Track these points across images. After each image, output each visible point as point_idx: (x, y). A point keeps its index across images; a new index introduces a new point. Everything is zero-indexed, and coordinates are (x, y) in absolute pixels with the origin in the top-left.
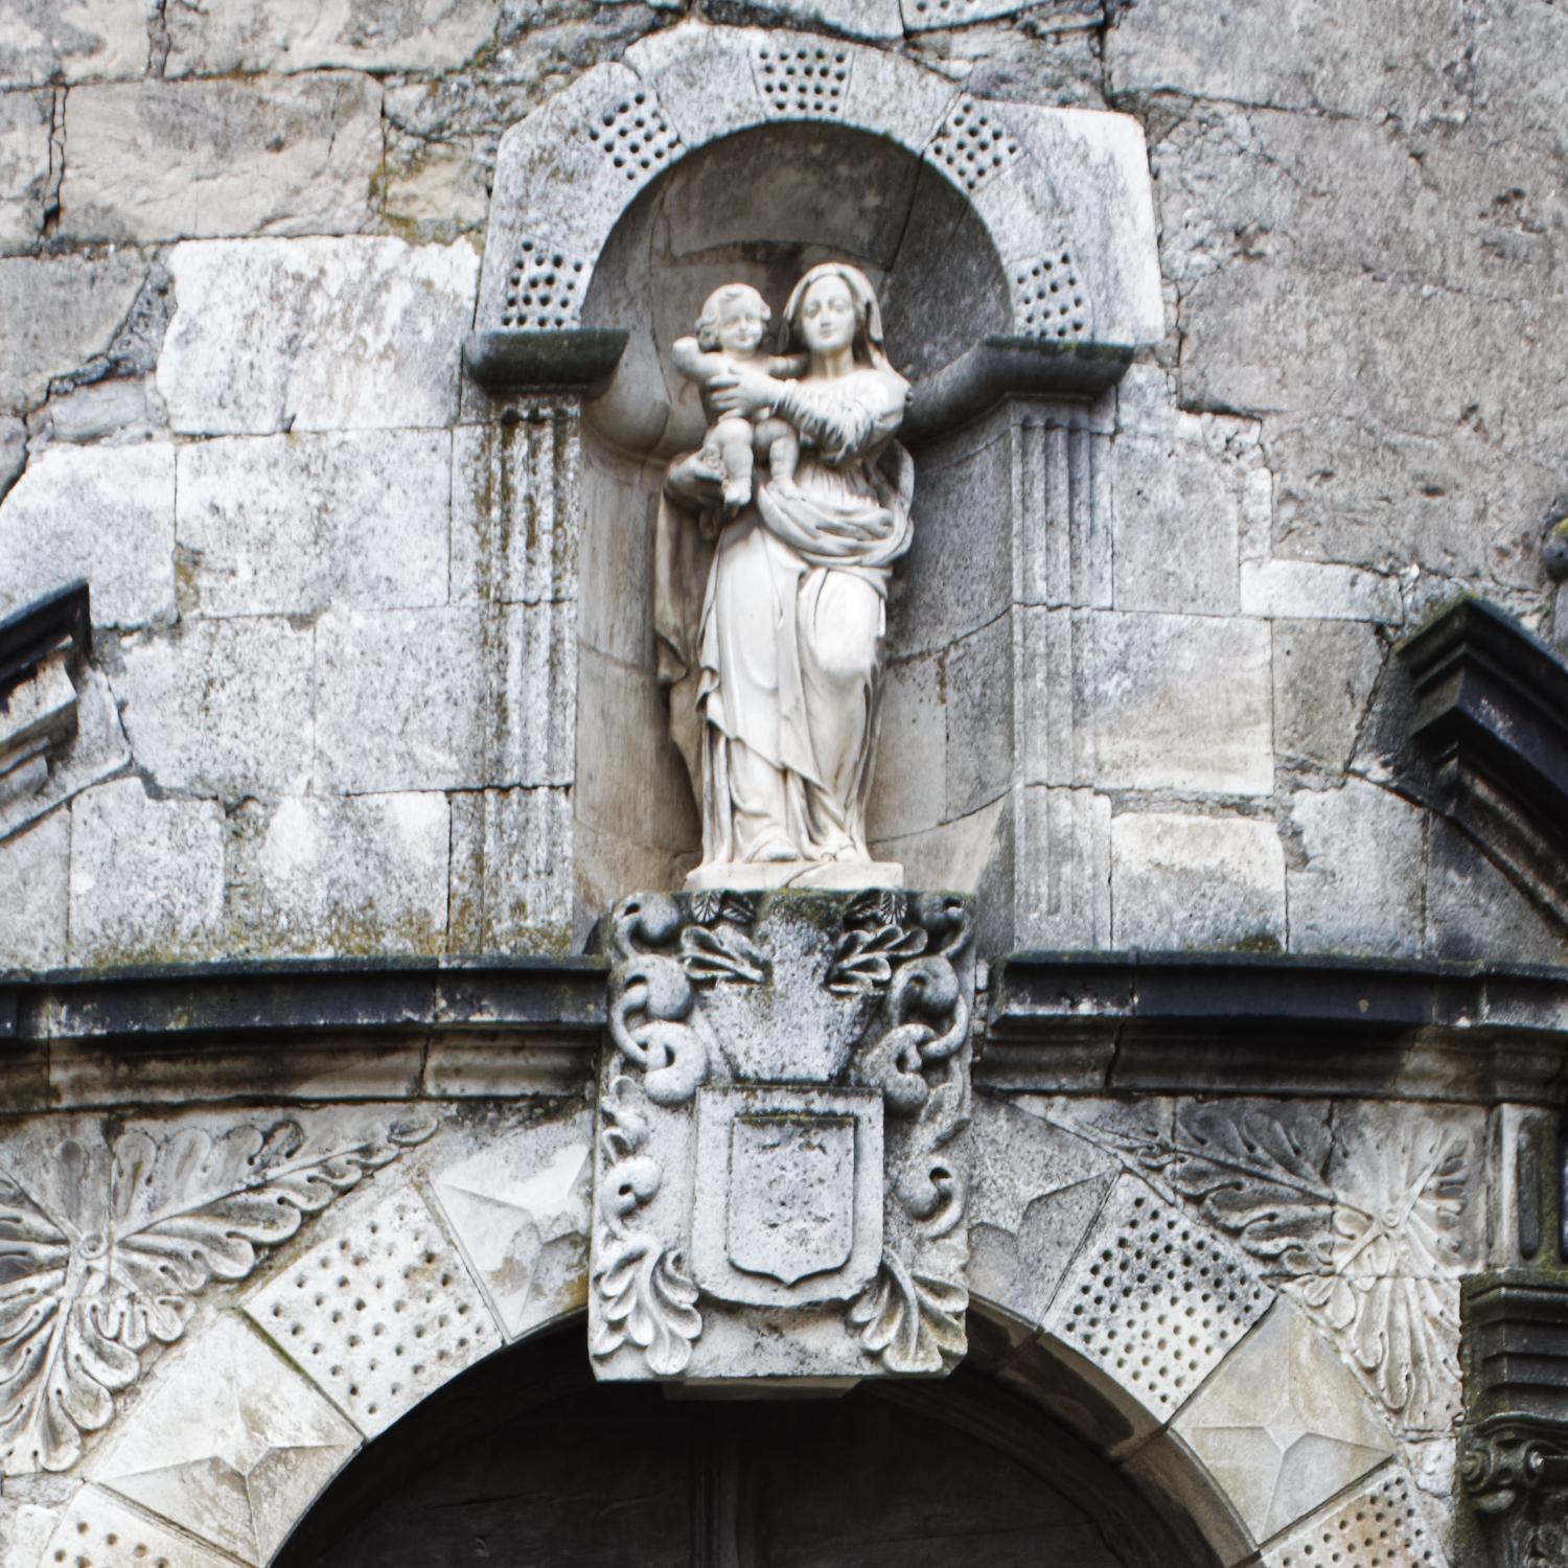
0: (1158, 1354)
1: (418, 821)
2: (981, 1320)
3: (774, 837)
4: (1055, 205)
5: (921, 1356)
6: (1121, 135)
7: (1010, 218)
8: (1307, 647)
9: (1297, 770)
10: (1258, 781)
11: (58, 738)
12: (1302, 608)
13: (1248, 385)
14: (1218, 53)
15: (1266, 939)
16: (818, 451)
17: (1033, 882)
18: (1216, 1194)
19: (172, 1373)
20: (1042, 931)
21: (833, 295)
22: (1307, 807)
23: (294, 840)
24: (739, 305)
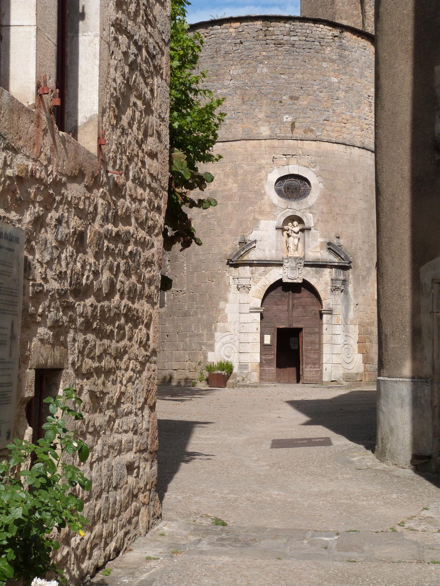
0: (313, 281)
1: (274, 251)
2: (304, 280)
3: (292, 253)
4: (307, 219)
5: (301, 281)
6: (311, 215)
7: (305, 220)
8: (322, 243)
9: (321, 249)
10: (319, 250)
11: (255, 247)
12: (321, 241)
13: (319, 229)
14: (317, 210)
15: (319, 259)
16: (294, 232)
17: (306, 256)
18: (317, 272)
19: (261, 280)
20: (307, 259)
21: (295, 223)
22: (322, 251)
23: (267, 252)
24: (290, 224)
